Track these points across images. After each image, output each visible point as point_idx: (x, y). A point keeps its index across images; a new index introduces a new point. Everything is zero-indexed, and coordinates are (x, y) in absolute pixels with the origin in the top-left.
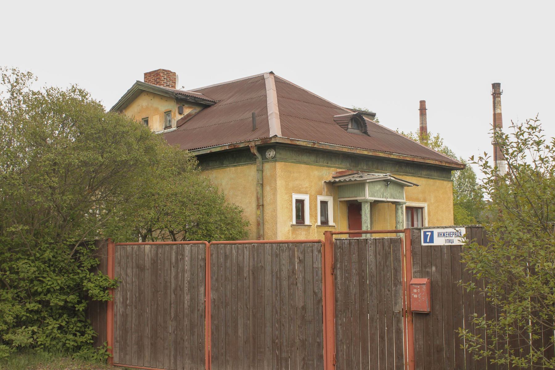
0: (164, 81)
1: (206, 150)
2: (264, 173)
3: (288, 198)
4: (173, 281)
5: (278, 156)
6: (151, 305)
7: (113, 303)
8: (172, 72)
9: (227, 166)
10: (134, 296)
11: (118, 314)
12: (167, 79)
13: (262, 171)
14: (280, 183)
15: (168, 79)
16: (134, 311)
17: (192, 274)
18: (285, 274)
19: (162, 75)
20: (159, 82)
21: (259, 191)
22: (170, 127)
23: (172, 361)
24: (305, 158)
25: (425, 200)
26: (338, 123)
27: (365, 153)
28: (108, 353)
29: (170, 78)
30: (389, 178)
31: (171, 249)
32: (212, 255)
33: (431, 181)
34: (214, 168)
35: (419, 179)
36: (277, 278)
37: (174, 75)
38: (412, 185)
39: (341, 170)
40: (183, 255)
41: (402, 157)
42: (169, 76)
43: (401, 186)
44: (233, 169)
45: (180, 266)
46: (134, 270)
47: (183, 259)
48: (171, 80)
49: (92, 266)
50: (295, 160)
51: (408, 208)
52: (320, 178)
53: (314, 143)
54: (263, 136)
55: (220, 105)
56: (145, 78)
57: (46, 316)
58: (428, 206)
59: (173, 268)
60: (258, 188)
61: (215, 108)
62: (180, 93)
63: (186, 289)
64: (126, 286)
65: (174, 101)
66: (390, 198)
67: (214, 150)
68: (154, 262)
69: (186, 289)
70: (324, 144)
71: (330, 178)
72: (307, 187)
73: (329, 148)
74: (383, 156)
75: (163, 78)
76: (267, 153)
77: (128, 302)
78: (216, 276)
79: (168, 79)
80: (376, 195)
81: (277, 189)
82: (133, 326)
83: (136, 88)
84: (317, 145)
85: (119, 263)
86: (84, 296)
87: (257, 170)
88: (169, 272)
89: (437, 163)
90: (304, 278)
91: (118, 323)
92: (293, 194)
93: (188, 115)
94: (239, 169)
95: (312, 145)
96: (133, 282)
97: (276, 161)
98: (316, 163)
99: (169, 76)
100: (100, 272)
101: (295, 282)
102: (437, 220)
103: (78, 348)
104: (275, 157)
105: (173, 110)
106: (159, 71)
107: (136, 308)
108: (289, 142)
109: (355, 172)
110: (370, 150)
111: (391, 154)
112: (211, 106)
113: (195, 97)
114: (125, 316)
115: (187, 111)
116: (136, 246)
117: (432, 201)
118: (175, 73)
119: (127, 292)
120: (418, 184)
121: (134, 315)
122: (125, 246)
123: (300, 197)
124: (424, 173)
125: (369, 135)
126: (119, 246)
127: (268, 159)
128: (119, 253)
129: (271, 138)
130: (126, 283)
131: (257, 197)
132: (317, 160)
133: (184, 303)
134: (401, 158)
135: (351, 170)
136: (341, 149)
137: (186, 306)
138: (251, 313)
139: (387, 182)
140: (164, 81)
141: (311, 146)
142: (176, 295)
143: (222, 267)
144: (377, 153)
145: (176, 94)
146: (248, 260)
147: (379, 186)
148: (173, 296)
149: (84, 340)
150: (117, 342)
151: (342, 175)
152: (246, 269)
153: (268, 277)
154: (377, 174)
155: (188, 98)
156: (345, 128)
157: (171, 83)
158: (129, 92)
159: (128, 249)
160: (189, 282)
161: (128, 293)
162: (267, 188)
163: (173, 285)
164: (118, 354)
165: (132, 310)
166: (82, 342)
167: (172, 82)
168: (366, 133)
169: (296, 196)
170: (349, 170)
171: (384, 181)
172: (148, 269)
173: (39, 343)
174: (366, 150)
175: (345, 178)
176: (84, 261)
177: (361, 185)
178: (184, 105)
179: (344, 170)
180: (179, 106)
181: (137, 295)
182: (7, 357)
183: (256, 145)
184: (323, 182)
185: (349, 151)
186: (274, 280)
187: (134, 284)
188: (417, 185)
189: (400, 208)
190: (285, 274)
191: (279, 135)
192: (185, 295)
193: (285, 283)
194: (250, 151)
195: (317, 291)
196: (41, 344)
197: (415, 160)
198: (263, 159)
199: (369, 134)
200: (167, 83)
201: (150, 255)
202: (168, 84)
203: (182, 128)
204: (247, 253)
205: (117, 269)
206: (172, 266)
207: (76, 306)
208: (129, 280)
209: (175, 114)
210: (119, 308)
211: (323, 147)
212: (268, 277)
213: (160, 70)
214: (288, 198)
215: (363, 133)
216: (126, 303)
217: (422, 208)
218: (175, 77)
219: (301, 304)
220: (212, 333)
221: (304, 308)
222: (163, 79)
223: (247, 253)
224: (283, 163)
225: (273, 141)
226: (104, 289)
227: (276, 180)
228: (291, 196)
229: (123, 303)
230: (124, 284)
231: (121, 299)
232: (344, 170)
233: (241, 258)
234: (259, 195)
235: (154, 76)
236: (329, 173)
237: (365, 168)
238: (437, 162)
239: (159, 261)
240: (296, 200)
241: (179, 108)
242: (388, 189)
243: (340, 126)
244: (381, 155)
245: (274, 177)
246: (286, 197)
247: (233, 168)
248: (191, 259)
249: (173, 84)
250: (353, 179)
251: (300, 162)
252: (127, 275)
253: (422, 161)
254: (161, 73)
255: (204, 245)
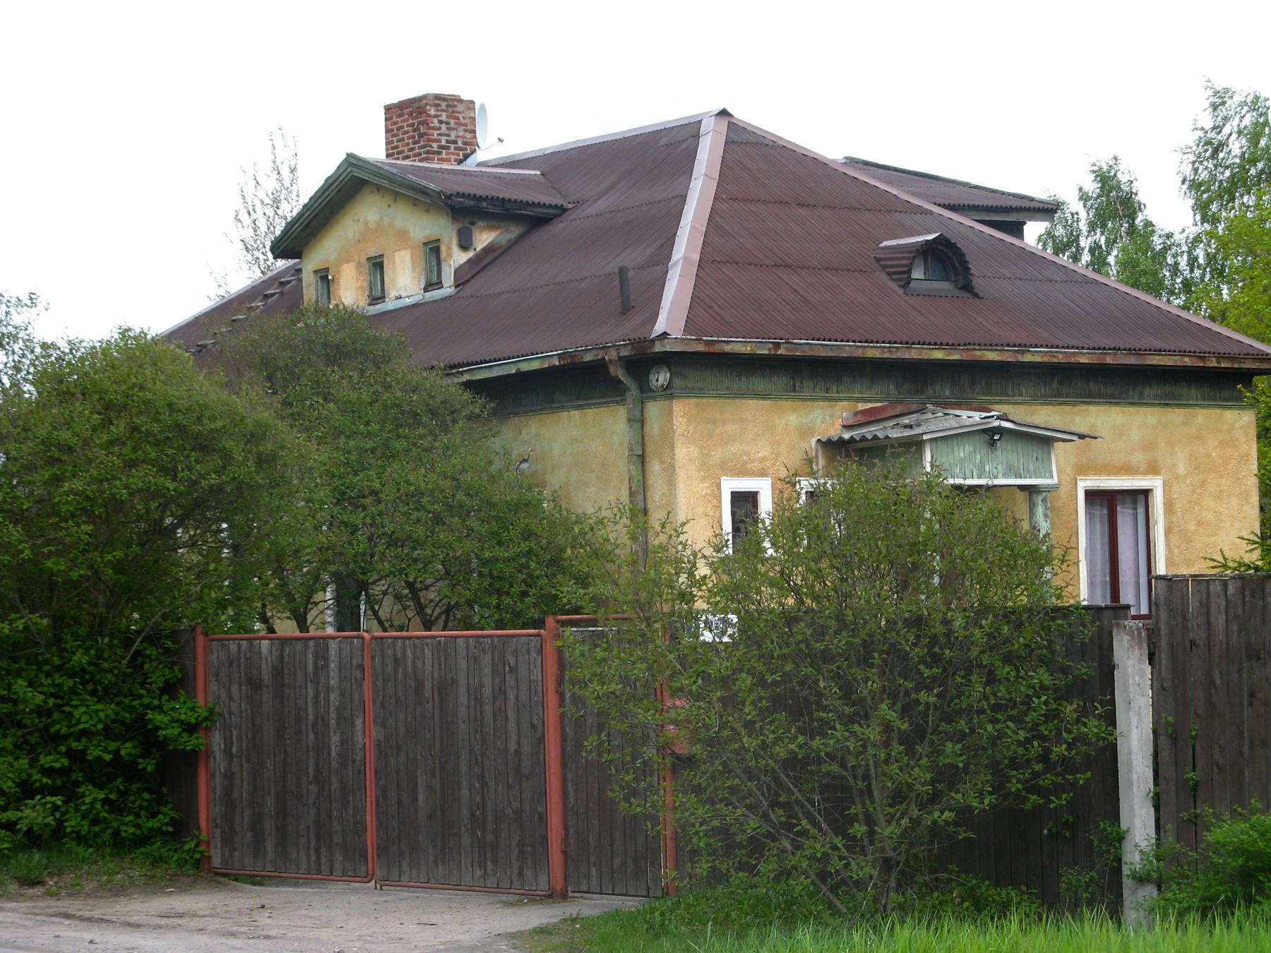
0: (440, 129)
1: (508, 367)
2: (647, 428)
3: (708, 491)
4: (310, 709)
5: (677, 382)
6: (275, 755)
7: (208, 753)
8: (461, 101)
9: (563, 408)
10: (245, 739)
11: (218, 773)
12: (448, 123)
13: (642, 423)
14: (684, 453)
15: (452, 122)
16: (245, 766)
17: (342, 695)
18: (487, 692)
19: (432, 112)
20: (426, 134)
21: (634, 473)
22: (439, 284)
23: (313, 858)
24: (759, 384)
25: (1153, 470)
26: (884, 267)
27: (939, 355)
28: (202, 848)
29: (458, 118)
30: (996, 423)
31: (306, 646)
32: (373, 658)
33: (1176, 415)
34: (532, 411)
35: (1132, 409)
36: (476, 699)
37: (469, 109)
38: (1075, 438)
39: (869, 406)
40: (326, 659)
41: (1061, 356)
42: (453, 112)
43: (1043, 441)
44: (576, 414)
45: (322, 679)
46: (243, 688)
47: (327, 666)
48: (459, 124)
49: (167, 681)
50: (728, 389)
51: (1091, 495)
52: (804, 432)
53: (777, 346)
54: (636, 335)
55: (572, 217)
56: (387, 120)
57: (80, 779)
58: (1165, 484)
59: (309, 684)
60: (632, 467)
61: (561, 226)
62: (458, 193)
63: (333, 722)
64: (230, 719)
65: (448, 214)
66: (1005, 476)
67: (525, 367)
68: (278, 672)
69: (333, 722)
70: (807, 344)
71: (834, 430)
72: (764, 459)
73: (824, 354)
74: (998, 358)
75: (436, 120)
76: (651, 377)
77: (234, 749)
78: (381, 697)
79: (452, 122)
80: (957, 471)
81: (677, 470)
82: (244, 795)
83: (345, 174)
84: (786, 349)
85: (217, 675)
86: (149, 739)
87: (629, 420)
88: (304, 691)
89: (1188, 361)
90: (517, 699)
91: (218, 790)
92: (724, 478)
93: (488, 250)
94: (591, 413)
95: (769, 349)
96: (241, 712)
97: (671, 397)
98: (792, 392)
99: (453, 112)
100: (182, 692)
101: (503, 707)
102: (1200, 524)
103: (141, 840)
104: (669, 387)
105: (445, 240)
106: (425, 102)
107: (248, 760)
108: (701, 348)
109: (914, 407)
110: (954, 346)
111: (1023, 352)
112: (551, 219)
113: (503, 199)
114: (229, 776)
115: (484, 239)
116: (245, 642)
117: (1181, 470)
118: (472, 102)
119: (231, 731)
120: (1097, 434)
121: (245, 774)
122: (226, 642)
123: (745, 484)
124: (1150, 392)
125: (977, 296)
126: (215, 643)
127: (653, 391)
128: (215, 655)
129: (653, 341)
130: (230, 713)
131: (630, 488)
132: (794, 386)
133: (329, 749)
134: (1060, 358)
135: (900, 402)
136: (859, 353)
137: (333, 754)
138: (437, 765)
139: (991, 436)
140: (440, 129)
141: (767, 352)
142: (316, 734)
143: (390, 680)
144: (978, 353)
145: (449, 197)
146: (430, 668)
147: (969, 448)
148: (311, 736)
149: (156, 825)
150: (217, 827)
151: (871, 417)
152: (428, 685)
153: (463, 699)
154: (964, 414)
155: (484, 205)
156: (900, 280)
157: (461, 134)
158: (329, 183)
159: (231, 647)
160: (337, 709)
161: (235, 733)
162: (655, 467)
163: (311, 717)
164: (219, 850)
165: (242, 766)
166: (151, 829)
167: (466, 131)
168: (967, 287)
169: (730, 485)
170: (893, 404)
171: (984, 431)
172: (267, 687)
173: (68, 830)
174: (940, 345)
175: (863, 431)
176: (152, 672)
177: (915, 445)
178: (473, 224)
179: (880, 404)
180: (461, 226)
181: (250, 736)
182: (8, 849)
183: (620, 358)
184: (814, 441)
185: (887, 355)
186: (472, 703)
187: (244, 715)
188: (1095, 438)
189: (1040, 502)
190: (487, 692)
191: (676, 333)
192: (332, 734)
193: (488, 709)
194: (608, 372)
195: (536, 722)
196: (73, 832)
197: (1109, 360)
198: (642, 392)
199: (976, 290)
200: (448, 135)
201: (269, 659)
202: (453, 137)
203: (469, 289)
204: (428, 653)
205: (214, 687)
206: (309, 680)
207: (140, 761)
208: (234, 706)
209: (449, 248)
210: (219, 762)
211: (804, 351)
212: (463, 699)
213: (425, 97)
214: (708, 491)
215: (961, 288)
216: (231, 750)
217: (1146, 493)
218: (472, 115)
219: (513, 747)
220: (377, 801)
221: (517, 752)
222: (438, 125)
223: (428, 653)
224: (693, 401)
225: (658, 348)
226: (191, 728)
227: (672, 448)
228: (719, 486)
229: (225, 751)
230: (227, 716)
231: (222, 745)
232: (880, 404)
233: (419, 664)
234: (633, 485)
235: (410, 114)
236: (832, 416)
237: (947, 393)
238: (1187, 359)
239: (286, 671)
240: (733, 493)
241: (460, 232)
242: (999, 453)
243: (889, 274)
244: (991, 356)
245: (668, 438)
246: (704, 488)
247: (577, 412)
248: (341, 667)
249: (468, 135)
250: (881, 435)
251: (741, 395)
252: (230, 697)
253: (1132, 360)
254: (431, 105)
255: (360, 640)
